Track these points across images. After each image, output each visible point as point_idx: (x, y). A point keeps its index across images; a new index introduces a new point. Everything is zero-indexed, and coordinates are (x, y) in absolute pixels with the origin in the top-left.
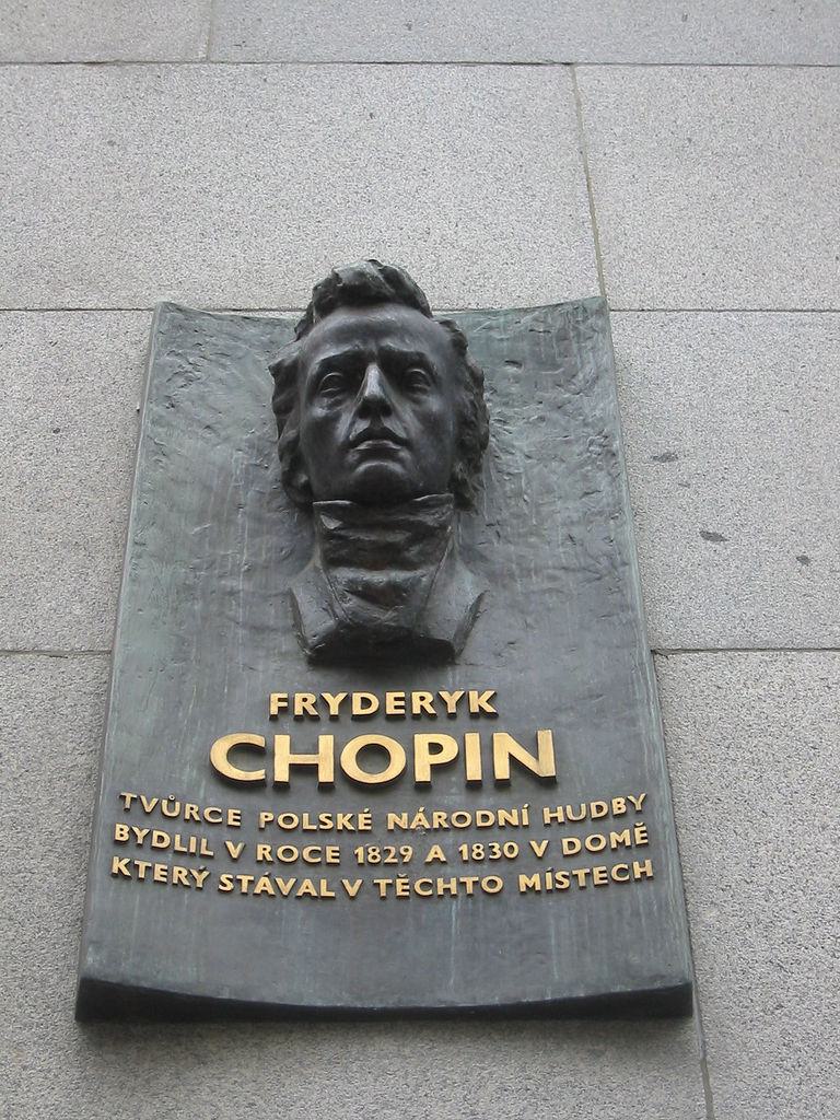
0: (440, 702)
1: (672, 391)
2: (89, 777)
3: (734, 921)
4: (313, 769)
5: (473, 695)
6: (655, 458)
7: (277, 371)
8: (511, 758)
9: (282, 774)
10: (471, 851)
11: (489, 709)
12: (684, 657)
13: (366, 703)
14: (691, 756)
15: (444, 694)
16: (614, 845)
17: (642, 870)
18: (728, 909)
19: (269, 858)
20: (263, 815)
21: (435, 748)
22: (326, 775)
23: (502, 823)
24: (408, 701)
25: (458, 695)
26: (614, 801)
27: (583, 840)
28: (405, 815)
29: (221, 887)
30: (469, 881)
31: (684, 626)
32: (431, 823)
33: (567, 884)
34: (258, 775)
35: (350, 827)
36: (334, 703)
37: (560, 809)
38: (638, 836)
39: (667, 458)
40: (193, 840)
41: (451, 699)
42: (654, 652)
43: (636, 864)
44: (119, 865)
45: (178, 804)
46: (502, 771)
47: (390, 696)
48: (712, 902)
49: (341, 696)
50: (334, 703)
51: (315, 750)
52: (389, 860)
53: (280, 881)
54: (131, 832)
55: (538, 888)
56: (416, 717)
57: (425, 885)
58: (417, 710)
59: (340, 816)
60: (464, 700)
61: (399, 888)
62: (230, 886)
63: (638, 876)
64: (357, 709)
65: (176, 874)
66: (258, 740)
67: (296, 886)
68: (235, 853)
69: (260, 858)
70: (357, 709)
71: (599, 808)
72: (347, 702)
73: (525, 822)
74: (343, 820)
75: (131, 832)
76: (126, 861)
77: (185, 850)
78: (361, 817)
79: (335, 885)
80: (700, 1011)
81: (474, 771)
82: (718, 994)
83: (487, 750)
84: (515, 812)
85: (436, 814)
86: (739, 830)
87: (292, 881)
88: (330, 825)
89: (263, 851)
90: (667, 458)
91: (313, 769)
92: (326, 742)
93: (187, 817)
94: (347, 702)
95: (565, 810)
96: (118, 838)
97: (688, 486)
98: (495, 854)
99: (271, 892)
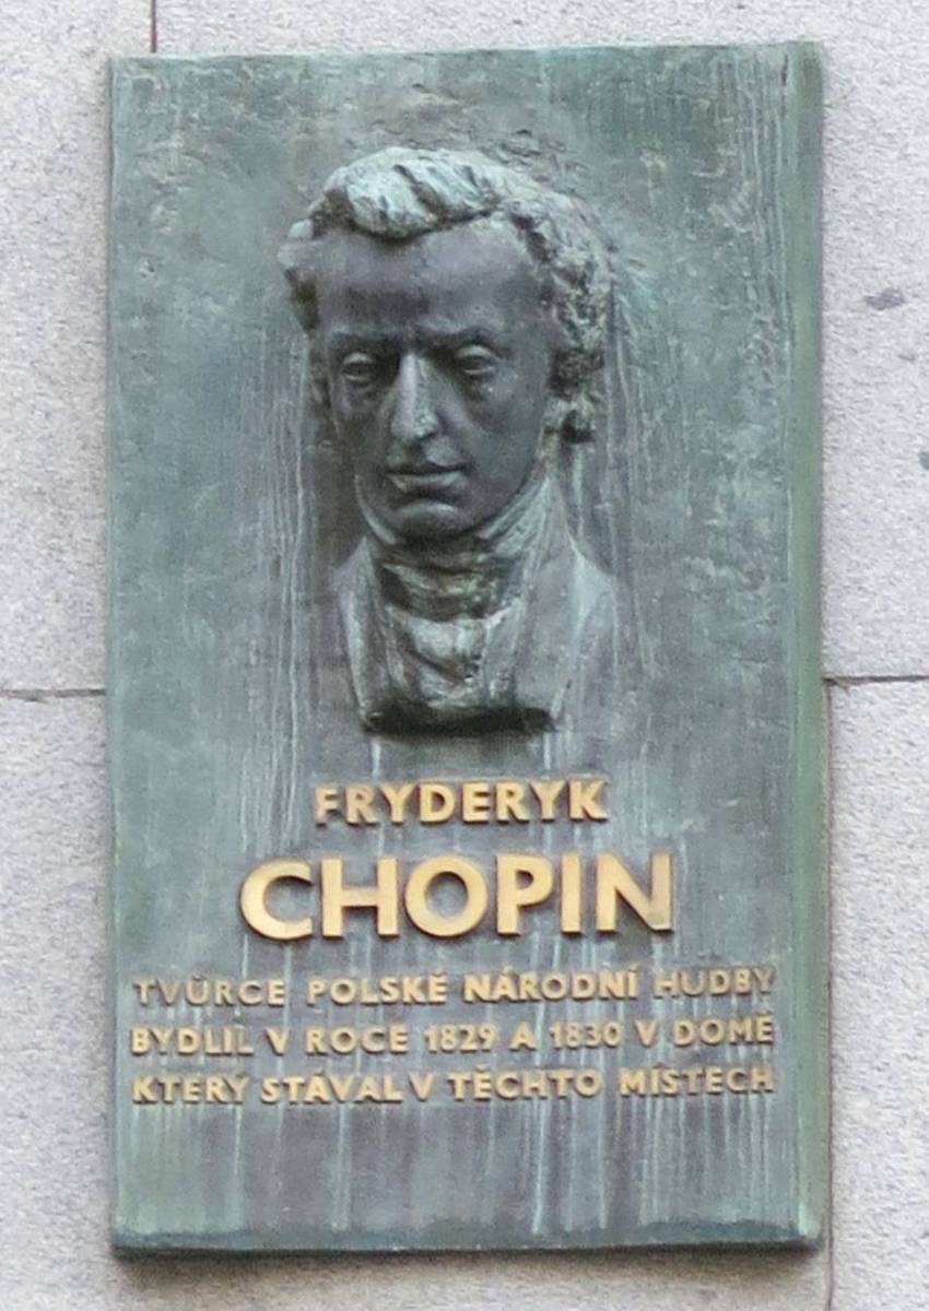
0: (534, 799)
1: (910, 150)
2: (95, 901)
3: (887, 1115)
4: (372, 912)
5: (576, 787)
6: (870, 301)
7: (291, 275)
8: (621, 898)
9: (333, 926)
10: (564, 1033)
11: (596, 813)
12: (869, 690)
13: (439, 799)
14: (861, 860)
15: (539, 788)
16: (733, 1039)
17: (760, 1079)
18: (881, 1097)
19: (322, 1048)
20: (312, 984)
21: (526, 877)
22: (389, 924)
23: (604, 993)
24: (491, 795)
25: (558, 786)
26: (738, 974)
27: (698, 1024)
28: (486, 979)
29: (267, 1098)
30: (562, 1076)
31: (876, 635)
32: (518, 992)
33: (675, 1086)
34: (303, 928)
35: (421, 998)
36: (398, 797)
37: (674, 976)
38: (762, 1029)
39: (887, 300)
40: (228, 1034)
41: (548, 793)
42: (830, 682)
43: (755, 1071)
44: (143, 1088)
45: (206, 984)
46: (607, 917)
47: (470, 789)
48: (864, 1089)
49: (407, 790)
50: (398, 797)
51: (372, 880)
52: (469, 1045)
53: (335, 1080)
54: (153, 1036)
55: (642, 1091)
56: (503, 823)
57: (511, 1082)
58: (503, 815)
59: (406, 981)
60: (564, 798)
61: (479, 1085)
62: (275, 1094)
63: (755, 1087)
64: (428, 813)
65: (210, 1089)
66: (302, 871)
67: (358, 1084)
68: (280, 1046)
69: (311, 1049)
70: (428, 813)
71: (720, 980)
72: (415, 799)
73: (632, 993)
74: (411, 989)
75: (153, 1036)
76: (149, 1080)
77: (217, 1050)
78: (433, 981)
79: (404, 1084)
80: (831, 1240)
81: (571, 922)
82: (856, 1218)
83: (590, 876)
84: (620, 977)
85: (524, 977)
86: (911, 980)
87: (350, 1079)
88: (394, 995)
89: (314, 1038)
90: (887, 300)
91: (372, 912)
92: (388, 869)
93: (219, 1000)
94: (415, 799)
95: (680, 976)
96: (137, 1049)
97: (912, 359)
98: (591, 1037)
99: (326, 1096)
